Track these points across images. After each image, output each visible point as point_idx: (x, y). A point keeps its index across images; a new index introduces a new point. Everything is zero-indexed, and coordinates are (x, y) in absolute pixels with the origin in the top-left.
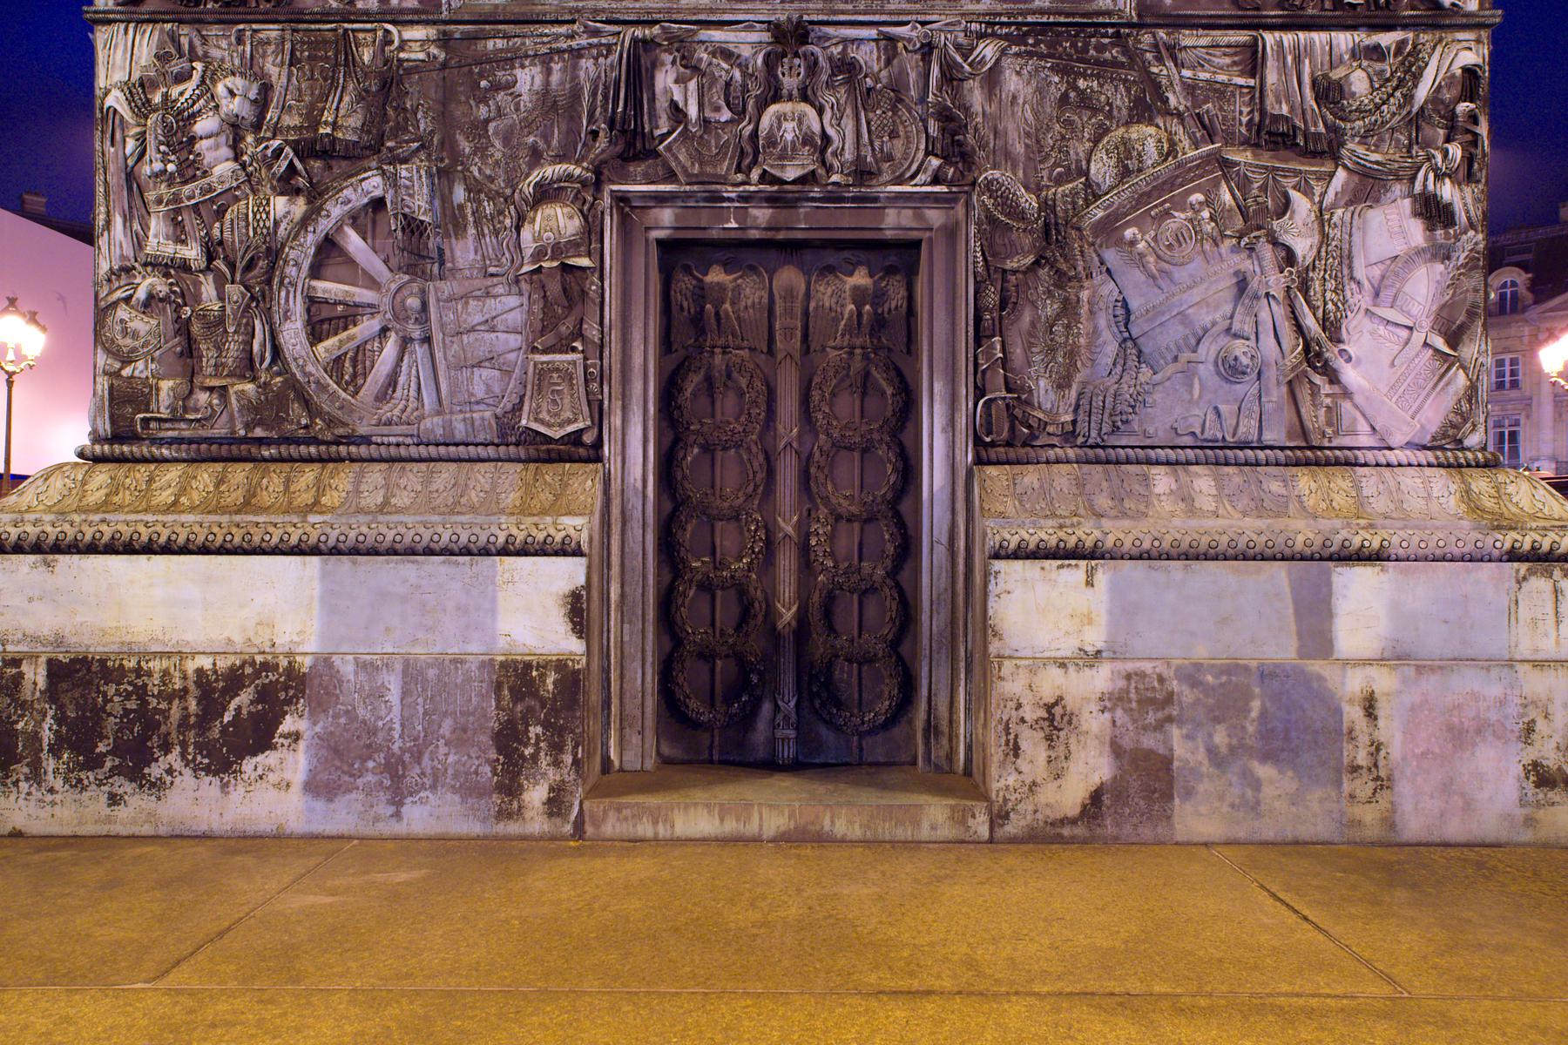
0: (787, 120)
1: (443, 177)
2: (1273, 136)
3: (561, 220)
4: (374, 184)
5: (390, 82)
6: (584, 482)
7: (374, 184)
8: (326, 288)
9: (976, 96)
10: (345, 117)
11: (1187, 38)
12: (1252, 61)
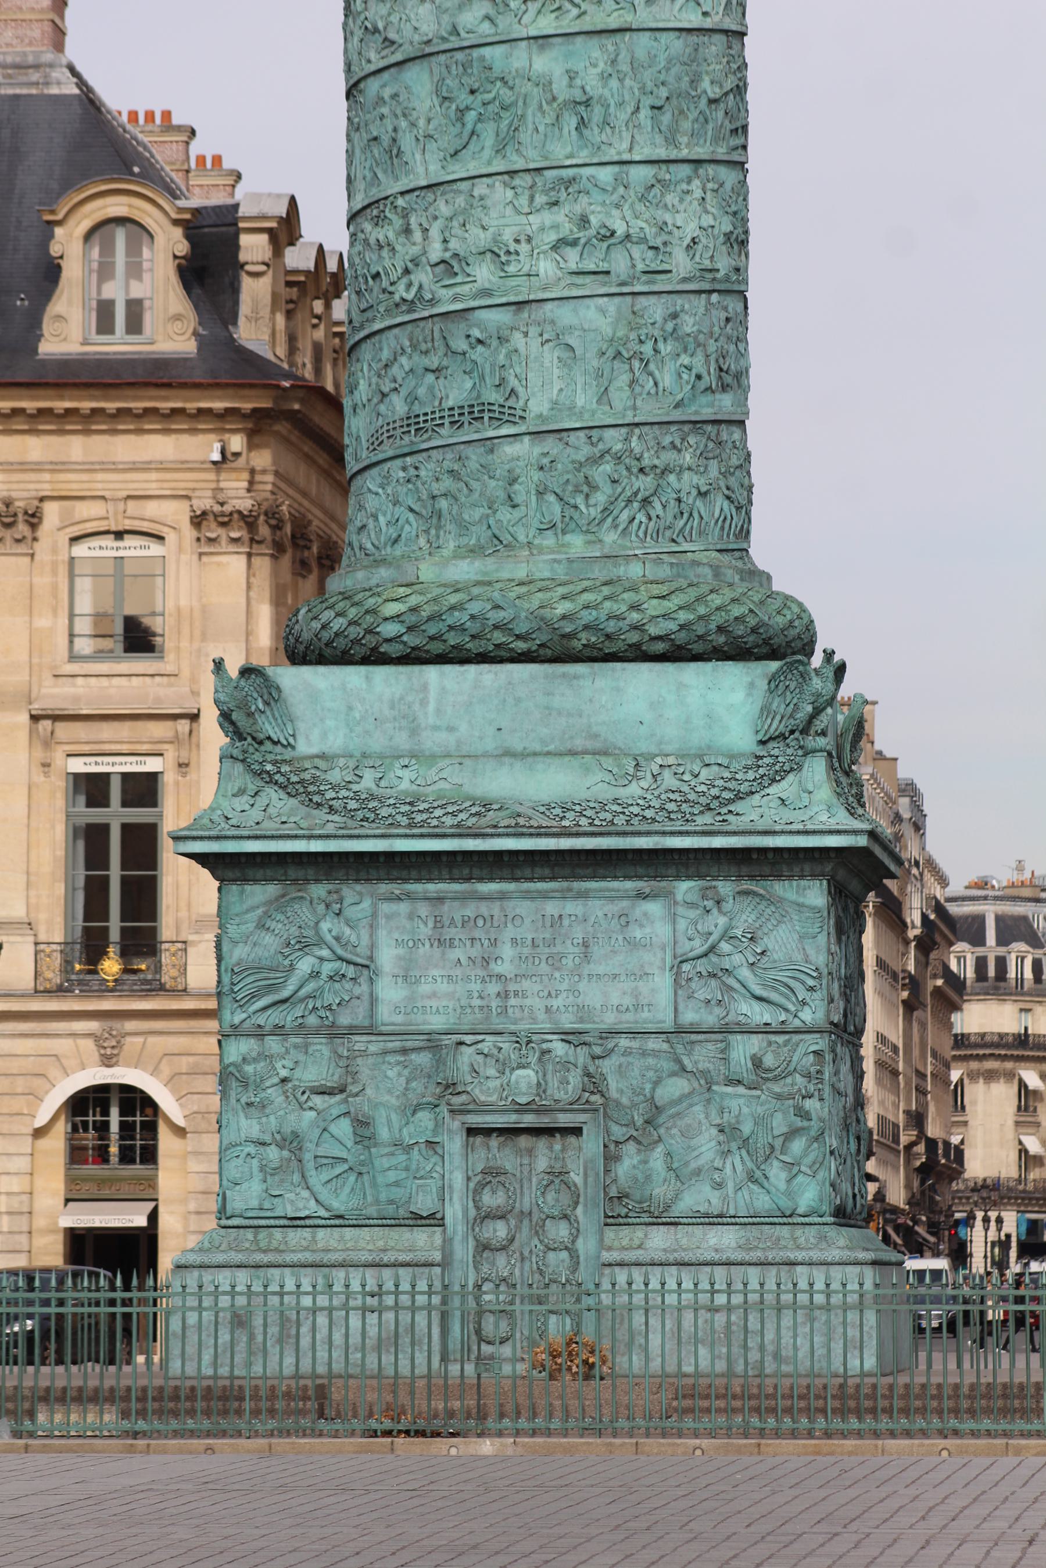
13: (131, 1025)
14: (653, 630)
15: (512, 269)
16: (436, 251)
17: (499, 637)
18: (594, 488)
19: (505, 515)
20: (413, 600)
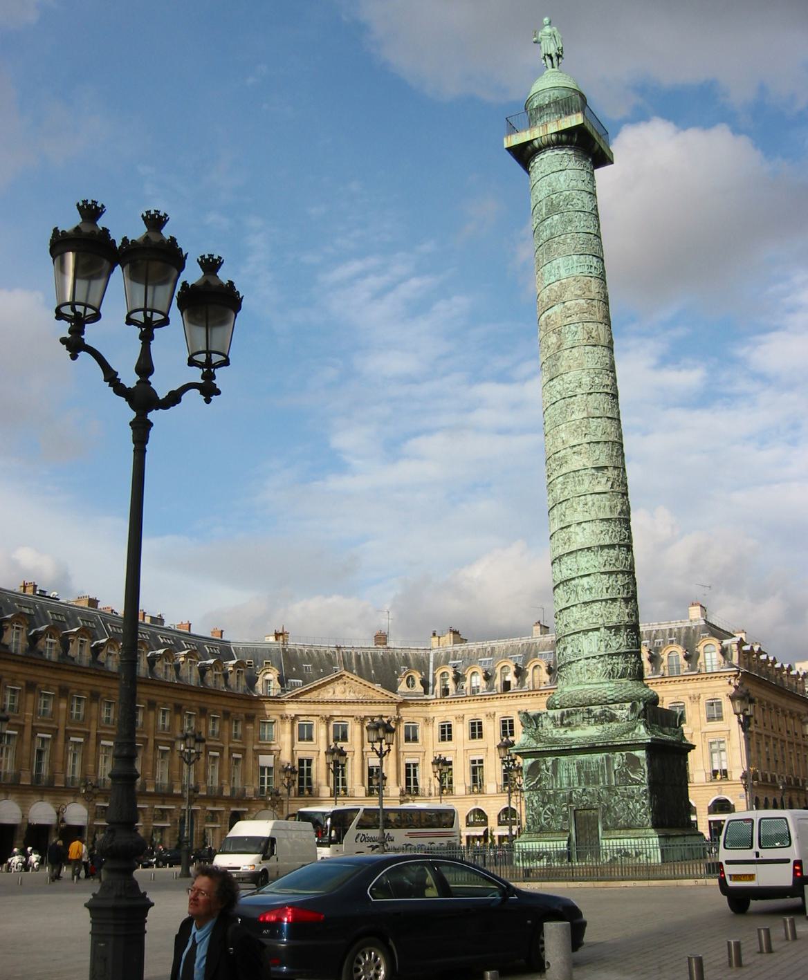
0: (584, 798)
2: (629, 797)
3: (565, 809)
4: (549, 806)
5: (549, 796)
7: (549, 806)
8: (545, 816)
9: (601, 795)
11: (620, 788)
12: (626, 789)
13: (723, 787)
14: (609, 698)
16: (565, 623)
17: (577, 702)
18: (598, 669)
19: (580, 676)
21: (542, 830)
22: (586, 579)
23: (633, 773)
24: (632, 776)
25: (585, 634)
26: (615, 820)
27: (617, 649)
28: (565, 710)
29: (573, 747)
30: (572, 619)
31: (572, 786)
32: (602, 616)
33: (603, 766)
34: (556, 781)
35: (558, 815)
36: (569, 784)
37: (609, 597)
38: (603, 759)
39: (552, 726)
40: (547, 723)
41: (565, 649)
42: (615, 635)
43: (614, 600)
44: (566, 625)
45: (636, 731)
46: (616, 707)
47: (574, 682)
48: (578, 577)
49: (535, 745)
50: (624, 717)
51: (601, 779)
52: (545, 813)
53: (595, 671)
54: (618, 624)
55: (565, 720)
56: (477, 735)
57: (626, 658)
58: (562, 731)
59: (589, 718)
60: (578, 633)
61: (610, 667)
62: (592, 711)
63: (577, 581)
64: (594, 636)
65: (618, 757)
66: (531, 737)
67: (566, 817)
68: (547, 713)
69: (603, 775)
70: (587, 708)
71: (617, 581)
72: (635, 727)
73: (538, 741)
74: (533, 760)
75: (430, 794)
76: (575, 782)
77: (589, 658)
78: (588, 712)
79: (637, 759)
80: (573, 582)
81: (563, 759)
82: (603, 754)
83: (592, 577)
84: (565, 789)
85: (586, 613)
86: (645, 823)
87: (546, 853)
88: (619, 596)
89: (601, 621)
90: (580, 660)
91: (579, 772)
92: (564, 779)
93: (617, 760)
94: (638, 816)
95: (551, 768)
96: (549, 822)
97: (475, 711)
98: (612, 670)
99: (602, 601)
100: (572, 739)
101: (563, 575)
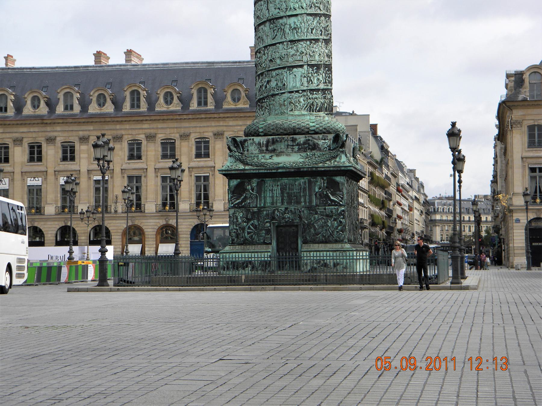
0: (287, 216)
1: (258, 221)
2: (327, 216)
5: (254, 213)
6: (270, 246)
8: (249, 230)
10: (249, 216)
12: (325, 209)
15: (284, 60)
17: (281, 131)
19: (283, 107)
20: (265, 125)
21: (245, 243)
22: (293, 19)
23: (333, 195)
24: (332, 198)
25: (290, 70)
26: (314, 236)
27: (317, 86)
28: (271, 137)
29: (279, 171)
30: (278, 55)
31: (275, 205)
32: (306, 54)
33: (305, 189)
34: (260, 200)
35: (261, 230)
36: (272, 203)
37: (312, 37)
38: (305, 182)
39: (257, 152)
40: (253, 149)
41: (268, 82)
42: (316, 72)
43: (317, 40)
44: (271, 61)
45: (338, 159)
46: (319, 137)
47: (276, 112)
48: (285, 17)
49: (242, 167)
50: (325, 146)
51: (302, 200)
52: (249, 228)
53: (297, 104)
54: (319, 63)
55: (270, 146)
56: (36, 158)
57: (324, 93)
58: (268, 156)
59: (293, 146)
60: (284, 68)
61: (311, 101)
62: (296, 139)
63: (284, 20)
64: (298, 72)
65: (320, 183)
66: (238, 160)
67: (268, 232)
68: (253, 140)
69: (305, 196)
70: (292, 136)
71: (320, 24)
72: (337, 156)
73: (245, 163)
74: (239, 180)
75: (116, 212)
76: (279, 201)
77: (292, 92)
78: (292, 141)
79: (337, 183)
80: (281, 21)
81: (269, 182)
82: (306, 178)
83: (299, 17)
84: (268, 207)
85: (292, 52)
86: (341, 238)
87: (250, 262)
88: (321, 37)
89: (305, 59)
90: (284, 93)
91: (282, 193)
92: (268, 198)
93: (318, 183)
94: (335, 233)
95: (255, 188)
96: (252, 236)
97: (34, 135)
98: (313, 104)
99: (307, 40)
100: (279, 163)
101: (271, 14)
